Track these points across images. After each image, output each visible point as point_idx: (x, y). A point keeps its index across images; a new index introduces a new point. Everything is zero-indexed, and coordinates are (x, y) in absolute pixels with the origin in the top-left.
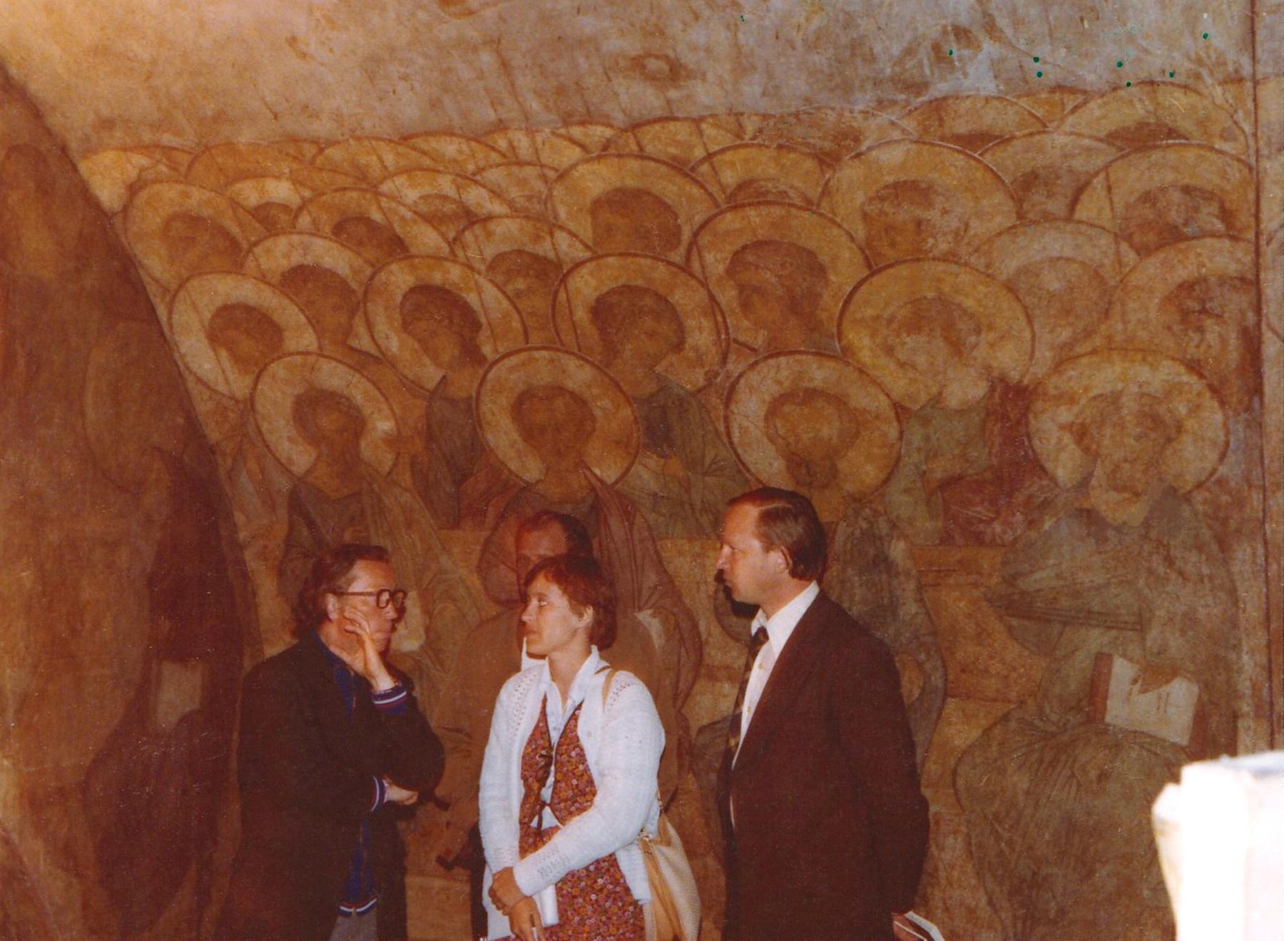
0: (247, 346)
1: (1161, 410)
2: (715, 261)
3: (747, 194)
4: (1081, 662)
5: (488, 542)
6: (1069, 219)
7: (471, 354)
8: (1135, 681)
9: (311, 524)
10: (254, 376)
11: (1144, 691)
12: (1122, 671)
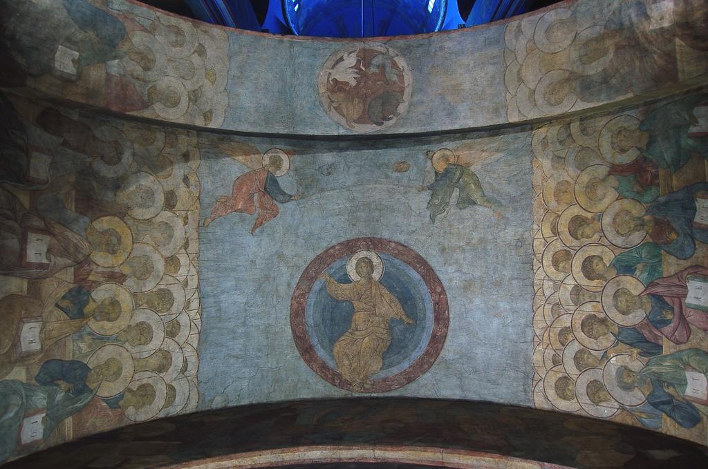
0: (602, 394)
1: (616, 132)
2: (575, 243)
3: (555, 232)
4: (690, 142)
5: (666, 337)
6: (565, 158)
7: (603, 321)
8: (695, 126)
9: (663, 403)
10: (612, 399)
11: (697, 122)
12: (693, 130)
